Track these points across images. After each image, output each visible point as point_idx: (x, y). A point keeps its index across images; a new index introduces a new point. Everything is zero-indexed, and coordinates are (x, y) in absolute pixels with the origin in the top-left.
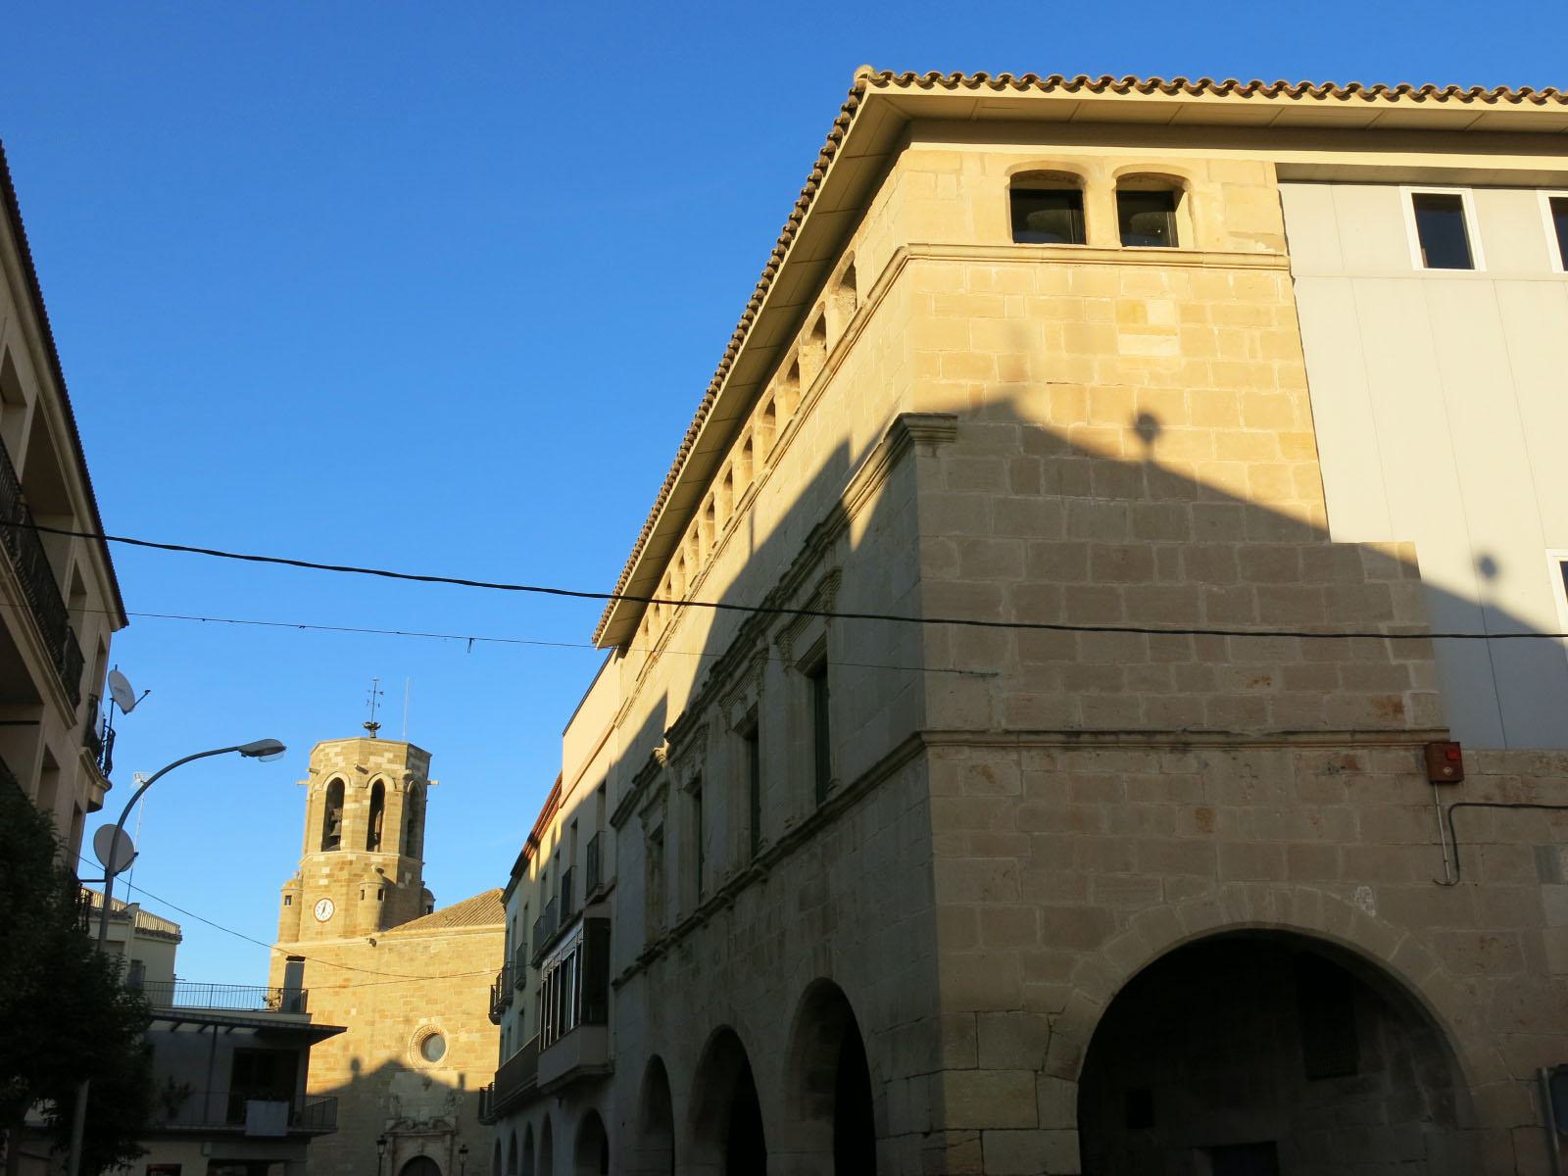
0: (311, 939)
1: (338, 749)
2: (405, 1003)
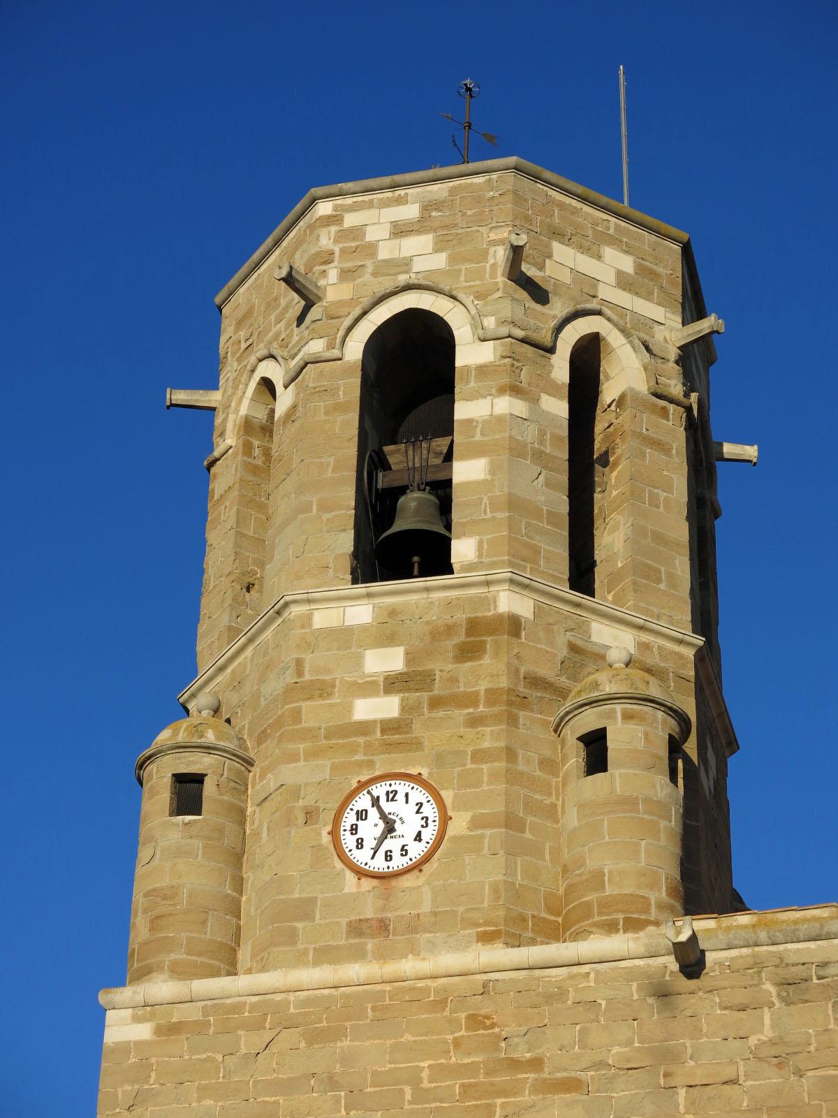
0: (326, 955)
1: (410, 212)
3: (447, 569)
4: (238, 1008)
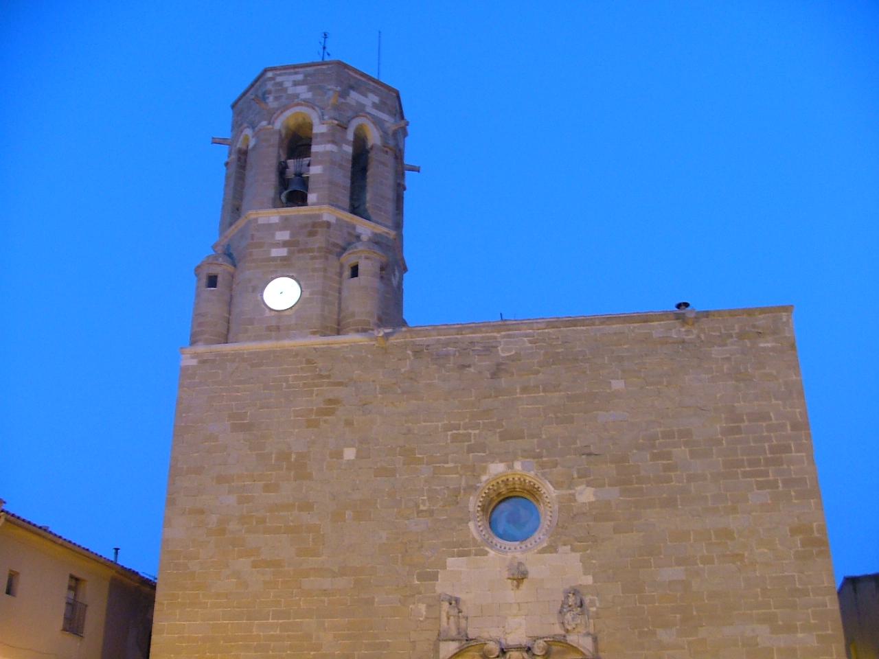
0: (259, 338)
2: (455, 439)
3: (306, 205)
4: (227, 355)
